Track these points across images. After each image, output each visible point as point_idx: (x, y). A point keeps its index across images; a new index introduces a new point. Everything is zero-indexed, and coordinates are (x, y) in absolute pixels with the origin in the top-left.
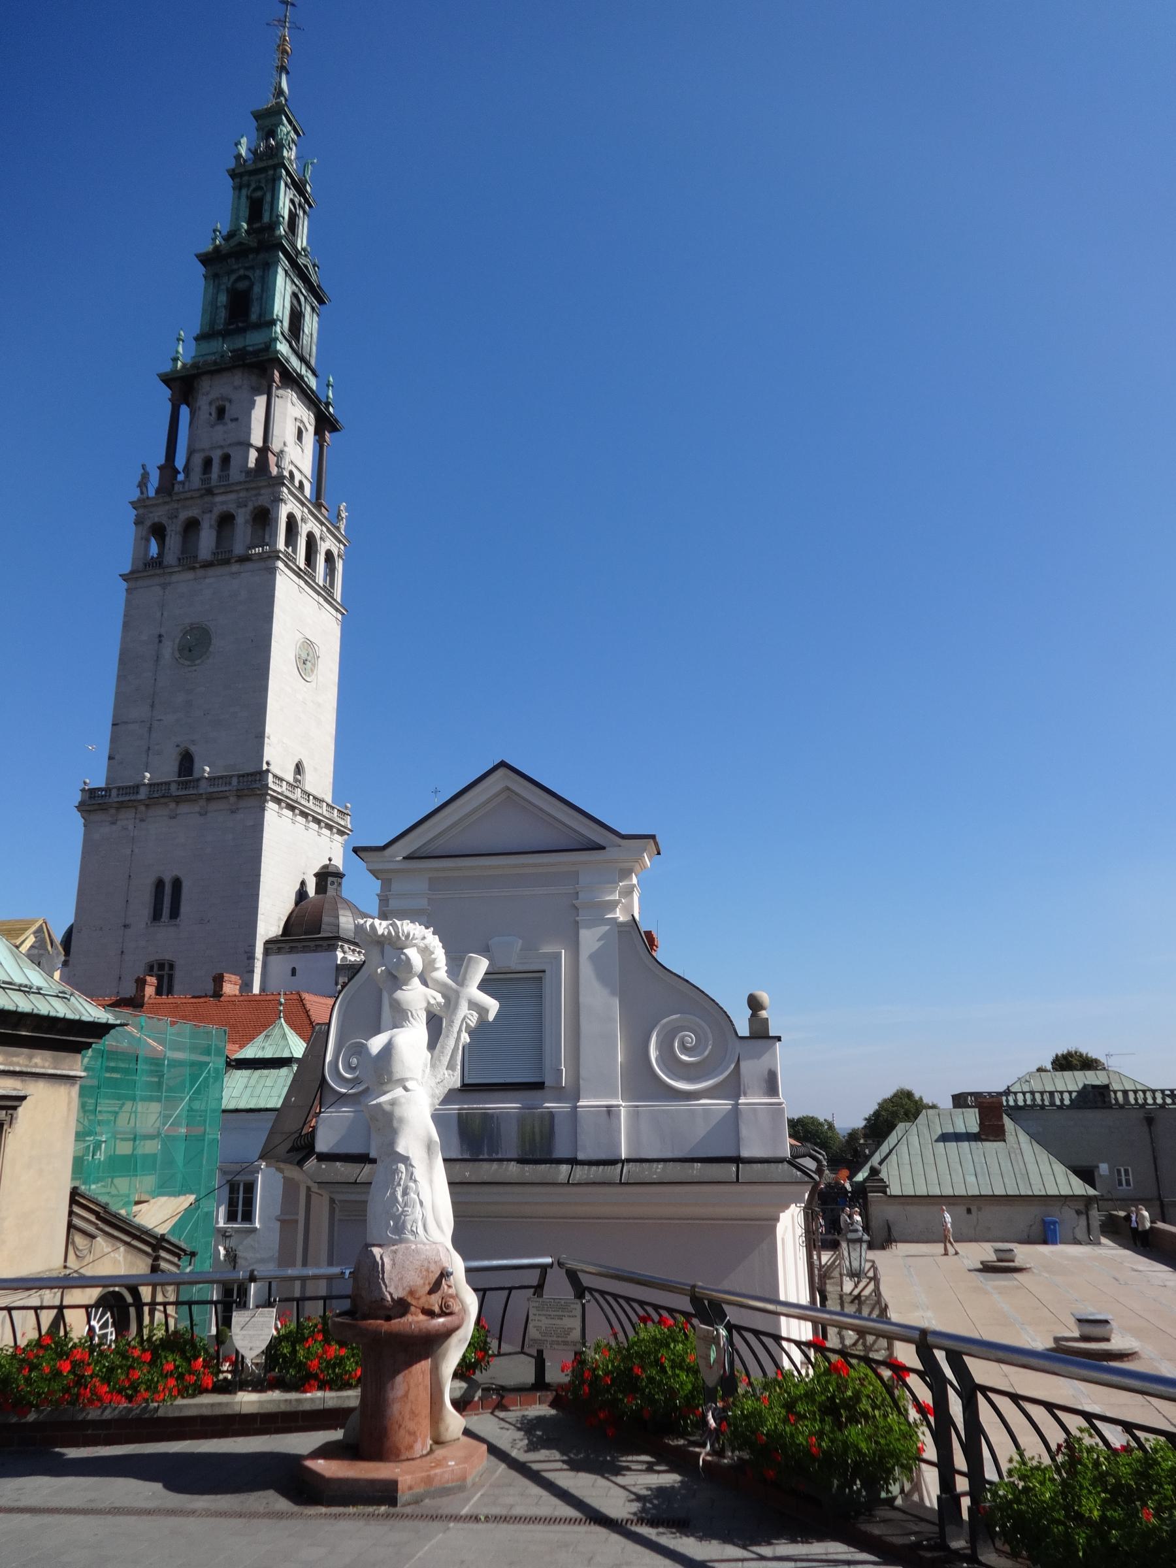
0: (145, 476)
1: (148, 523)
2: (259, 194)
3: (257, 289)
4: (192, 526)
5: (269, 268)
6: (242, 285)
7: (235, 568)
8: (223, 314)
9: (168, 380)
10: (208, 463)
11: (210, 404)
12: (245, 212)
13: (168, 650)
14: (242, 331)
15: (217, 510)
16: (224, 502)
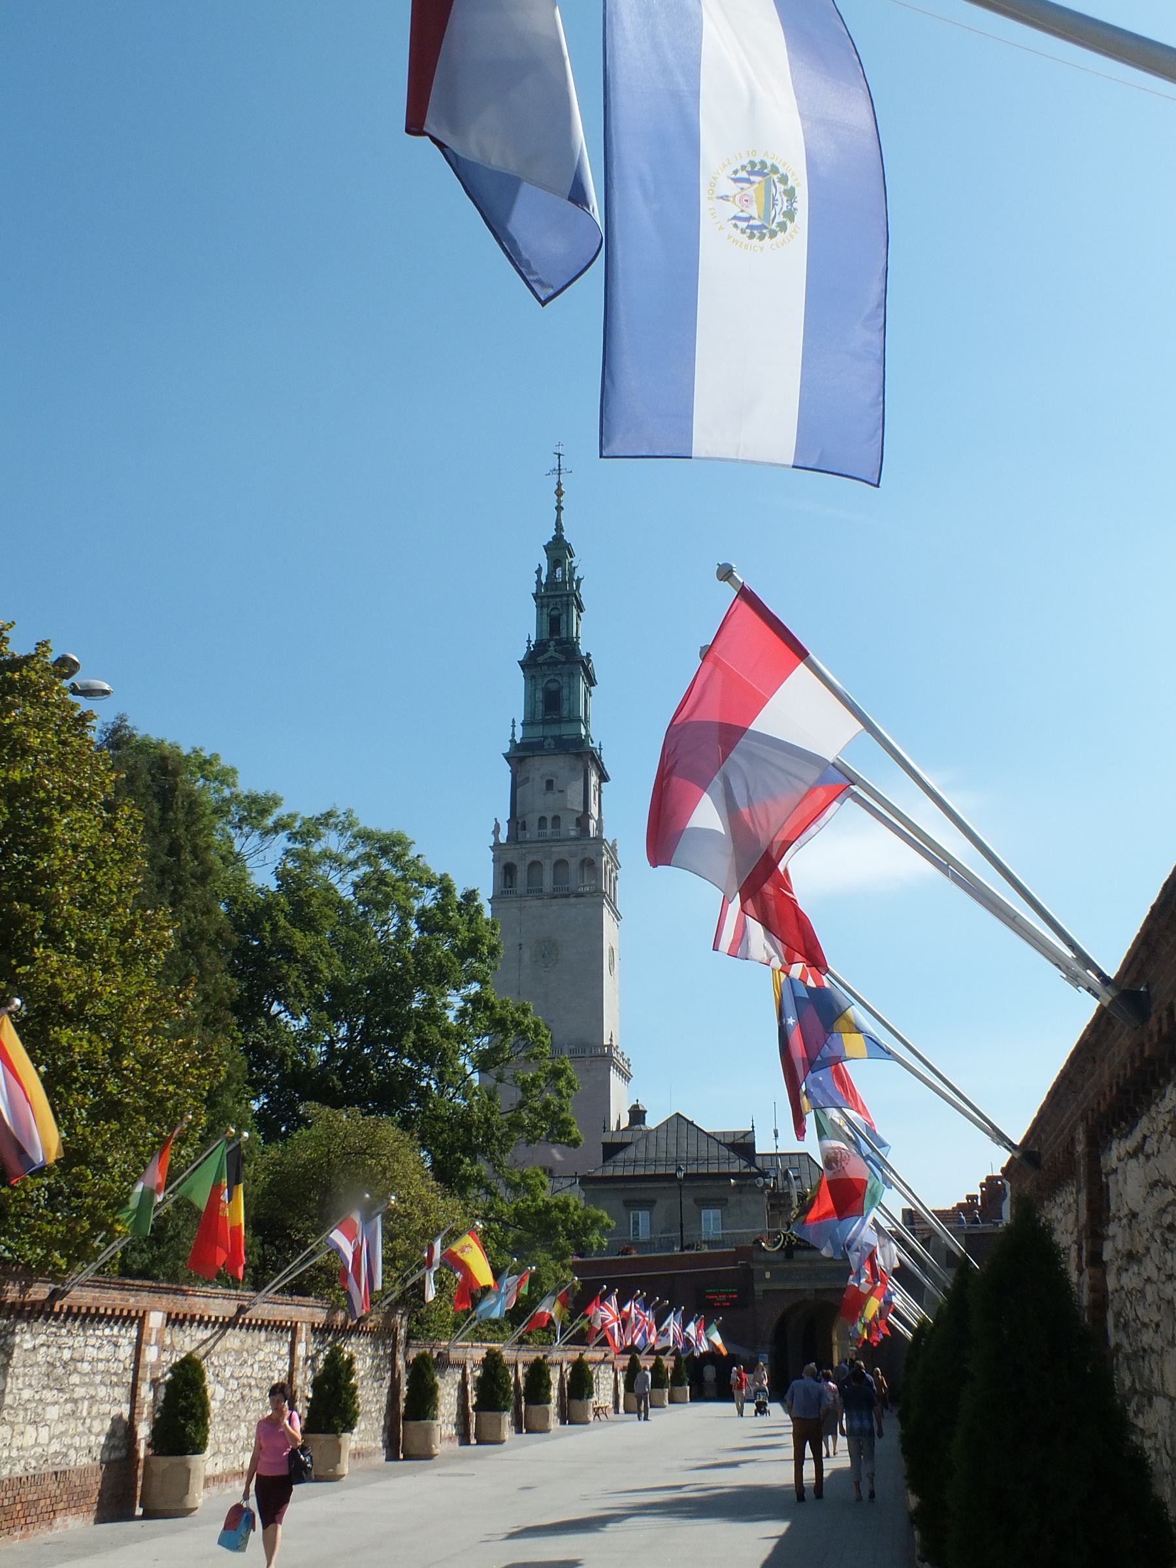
0: (497, 826)
1: (503, 863)
2: (555, 613)
3: (565, 692)
4: (535, 865)
5: (572, 675)
6: (553, 687)
7: (573, 900)
8: (540, 707)
9: (508, 757)
10: (542, 820)
11: (542, 778)
12: (546, 627)
13: (527, 955)
14: (559, 721)
15: (555, 858)
16: (560, 851)
